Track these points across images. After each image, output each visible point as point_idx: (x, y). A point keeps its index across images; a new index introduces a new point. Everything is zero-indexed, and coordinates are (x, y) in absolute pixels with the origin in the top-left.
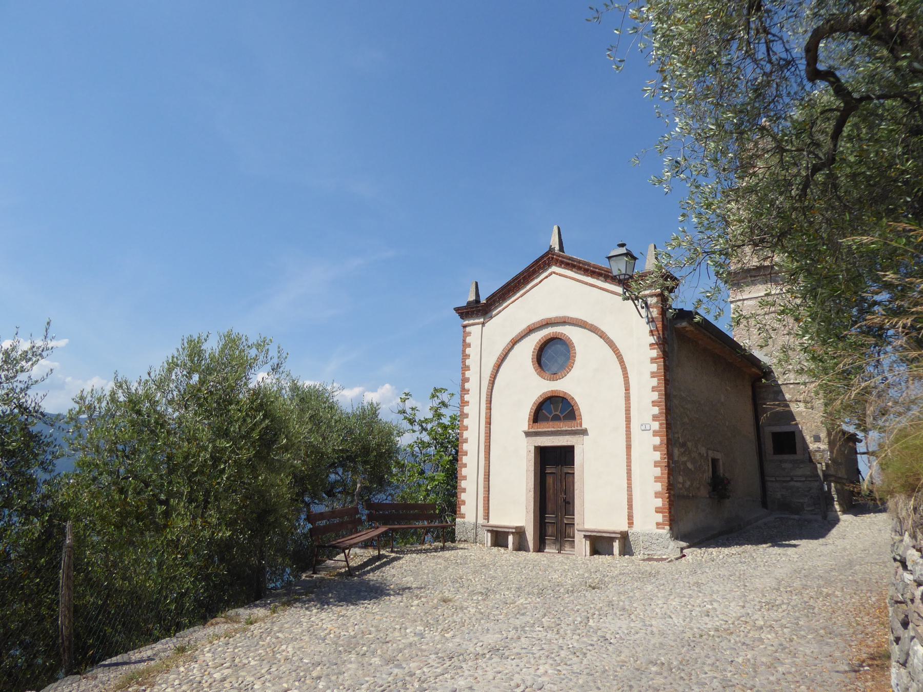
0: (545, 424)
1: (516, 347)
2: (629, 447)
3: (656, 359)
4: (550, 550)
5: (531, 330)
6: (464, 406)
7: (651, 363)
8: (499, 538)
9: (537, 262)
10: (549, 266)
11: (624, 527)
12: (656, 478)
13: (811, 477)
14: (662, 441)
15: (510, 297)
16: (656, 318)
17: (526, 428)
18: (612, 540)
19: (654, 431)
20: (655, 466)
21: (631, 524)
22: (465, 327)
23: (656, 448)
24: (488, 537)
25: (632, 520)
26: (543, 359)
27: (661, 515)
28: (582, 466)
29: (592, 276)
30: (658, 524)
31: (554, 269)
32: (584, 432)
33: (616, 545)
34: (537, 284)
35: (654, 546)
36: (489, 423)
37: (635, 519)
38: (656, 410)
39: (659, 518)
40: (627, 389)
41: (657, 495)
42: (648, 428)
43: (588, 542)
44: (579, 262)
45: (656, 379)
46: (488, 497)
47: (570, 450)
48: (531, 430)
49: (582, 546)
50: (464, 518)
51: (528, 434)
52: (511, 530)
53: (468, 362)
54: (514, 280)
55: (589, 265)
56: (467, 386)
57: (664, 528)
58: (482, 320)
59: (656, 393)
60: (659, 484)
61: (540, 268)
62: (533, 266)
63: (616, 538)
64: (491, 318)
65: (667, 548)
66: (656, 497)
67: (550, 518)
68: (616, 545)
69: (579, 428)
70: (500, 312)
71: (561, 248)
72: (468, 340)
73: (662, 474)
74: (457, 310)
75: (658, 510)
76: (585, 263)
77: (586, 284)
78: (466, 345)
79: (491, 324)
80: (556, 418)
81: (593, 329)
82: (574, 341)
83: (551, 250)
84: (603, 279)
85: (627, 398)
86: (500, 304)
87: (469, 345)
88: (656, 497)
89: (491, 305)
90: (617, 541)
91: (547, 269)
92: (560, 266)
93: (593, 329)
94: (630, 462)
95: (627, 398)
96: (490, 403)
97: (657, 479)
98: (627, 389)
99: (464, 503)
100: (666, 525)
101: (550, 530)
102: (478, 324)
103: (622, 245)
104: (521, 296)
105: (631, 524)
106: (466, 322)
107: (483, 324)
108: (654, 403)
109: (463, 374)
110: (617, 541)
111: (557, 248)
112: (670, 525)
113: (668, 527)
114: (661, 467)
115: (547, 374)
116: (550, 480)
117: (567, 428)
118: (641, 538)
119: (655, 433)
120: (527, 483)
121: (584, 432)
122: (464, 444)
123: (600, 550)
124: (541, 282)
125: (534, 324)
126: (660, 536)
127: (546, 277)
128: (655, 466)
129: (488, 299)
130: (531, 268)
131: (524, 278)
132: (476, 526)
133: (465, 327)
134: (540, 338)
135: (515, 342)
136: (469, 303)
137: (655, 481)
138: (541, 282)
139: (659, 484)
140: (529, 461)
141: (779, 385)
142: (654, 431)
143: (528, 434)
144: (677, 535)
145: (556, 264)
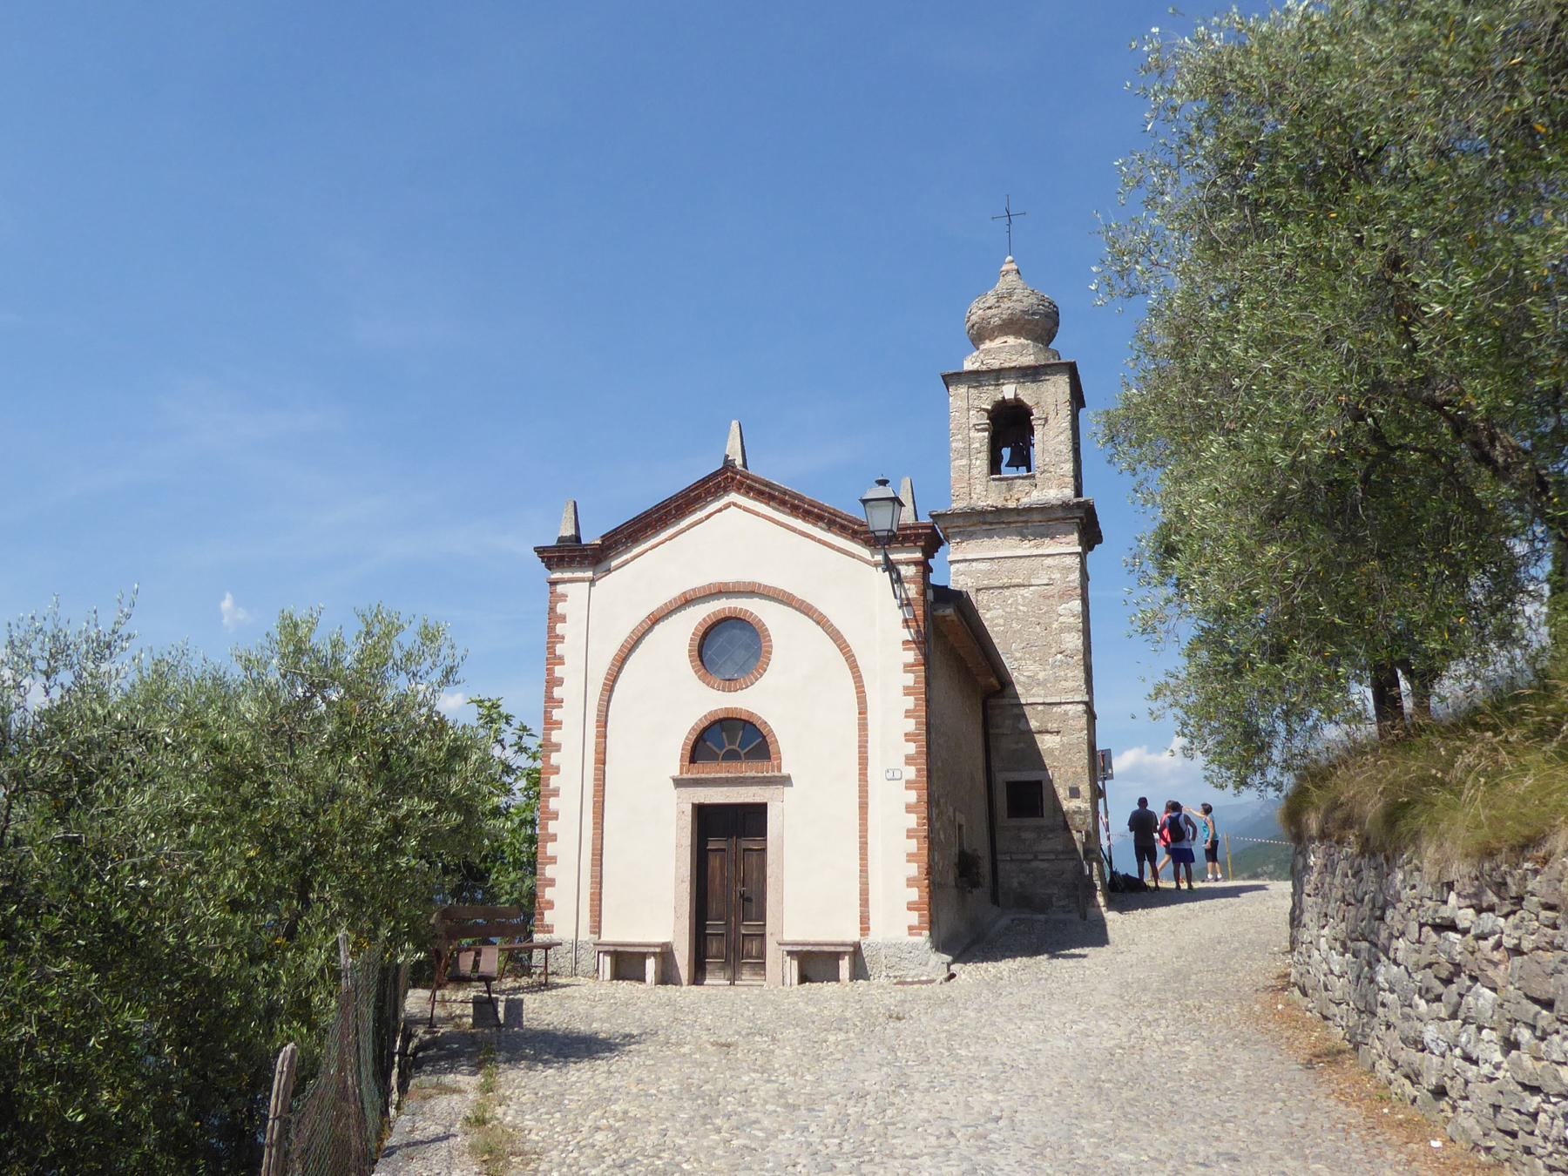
0: (712, 765)
1: (657, 627)
2: (864, 807)
4: (715, 982)
5: (687, 601)
7: (905, 672)
8: (626, 964)
9: (704, 481)
10: (726, 490)
11: (853, 935)
12: (908, 855)
14: (919, 796)
15: (647, 538)
16: (914, 599)
17: (676, 773)
18: (837, 956)
19: (907, 782)
20: (908, 837)
21: (865, 929)
22: (553, 583)
23: (909, 809)
24: (606, 963)
26: (708, 654)
27: (916, 914)
29: (804, 519)
30: (911, 928)
31: (734, 497)
32: (786, 781)
33: (845, 966)
34: (700, 521)
35: (903, 963)
36: (601, 761)
37: (872, 924)
38: (911, 748)
39: (914, 918)
40: (863, 712)
41: (911, 882)
42: (897, 775)
43: (795, 963)
44: (785, 492)
45: (912, 698)
46: (600, 894)
47: (761, 809)
48: (685, 776)
49: (781, 968)
50: (550, 932)
51: (679, 783)
52: (652, 950)
53: (560, 649)
54: (658, 508)
55: (801, 499)
56: (557, 692)
57: (920, 934)
58: (589, 574)
59: (912, 721)
60: (915, 865)
61: (708, 493)
62: (696, 488)
63: (845, 953)
64: (609, 571)
65: (926, 964)
67: (714, 926)
68: (845, 966)
69: (776, 774)
71: (745, 465)
73: (919, 849)
74: (540, 551)
75: (911, 907)
76: (795, 496)
77: (794, 530)
78: (554, 618)
79: (606, 583)
80: (732, 756)
81: (805, 609)
82: (768, 625)
83: (728, 465)
84: (824, 526)
85: (863, 727)
86: (628, 550)
87: (563, 619)
89: (609, 548)
90: (847, 958)
91: (721, 497)
92: (746, 494)
93: (805, 609)
94: (866, 831)
95: (863, 727)
96: (605, 726)
97: (911, 857)
98: (863, 712)
99: (550, 905)
100: (923, 929)
101: (714, 946)
102: (582, 580)
103: (883, 483)
104: (671, 538)
105: (865, 929)
106: (557, 575)
107: (592, 582)
108: (909, 737)
109: (550, 671)
110: (847, 958)
111: (739, 462)
112: (930, 930)
113: (926, 933)
114: (918, 838)
115: (718, 681)
116: (714, 862)
117: (753, 774)
118: (883, 952)
119: (909, 785)
120: (677, 868)
121: (786, 781)
122: (552, 799)
123: (810, 973)
124: (708, 517)
125: (694, 590)
126: (915, 946)
127: (720, 510)
128: (908, 837)
129: (605, 538)
130: (692, 491)
131: (678, 508)
132: (576, 946)
133: (553, 583)
135: (655, 619)
136: (561, 539)
137: (908, 861)
138: (708, 517)
139: (915, 865)
140: (680, 828)
141: (1021, 705)
142: (907, 782)
143: (679, 783)
144: (940, 945)
145: (738, 490)
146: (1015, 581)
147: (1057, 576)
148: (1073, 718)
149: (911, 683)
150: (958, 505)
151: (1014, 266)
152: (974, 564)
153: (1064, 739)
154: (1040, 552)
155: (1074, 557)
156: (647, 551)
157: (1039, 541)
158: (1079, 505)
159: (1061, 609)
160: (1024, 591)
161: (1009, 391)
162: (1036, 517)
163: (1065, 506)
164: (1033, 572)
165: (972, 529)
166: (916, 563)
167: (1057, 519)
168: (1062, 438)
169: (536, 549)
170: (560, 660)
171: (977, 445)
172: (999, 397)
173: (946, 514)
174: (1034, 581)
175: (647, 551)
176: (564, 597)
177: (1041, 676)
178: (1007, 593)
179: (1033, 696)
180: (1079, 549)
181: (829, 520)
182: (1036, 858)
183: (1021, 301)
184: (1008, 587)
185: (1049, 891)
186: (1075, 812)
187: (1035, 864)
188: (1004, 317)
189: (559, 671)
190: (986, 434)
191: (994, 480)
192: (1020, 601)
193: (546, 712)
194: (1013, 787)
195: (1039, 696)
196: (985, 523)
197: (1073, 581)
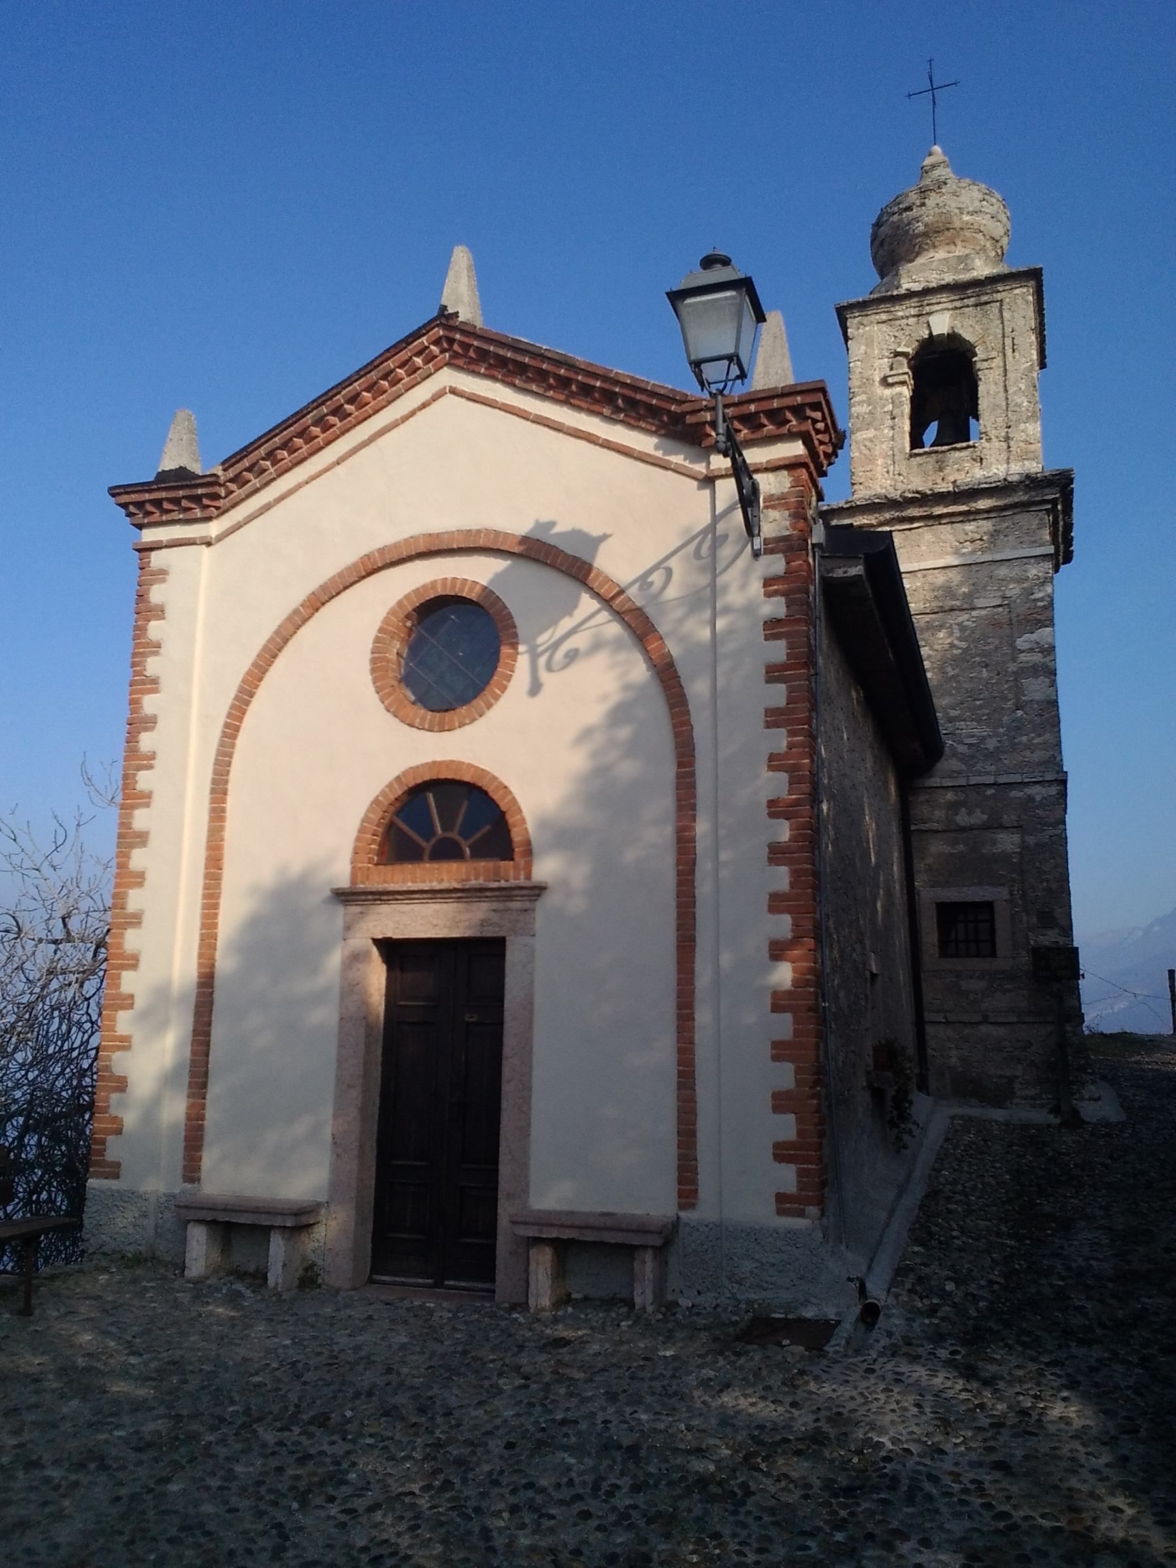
3: (784, 667)
6: (133, 807)
12: (776, 1045)
21: (687, 1192)
25: (694, 1181)
28: (528, 1004)
30: (781, 1198)
31: (447, 377)
34: (395, 425)
50: (117, 1176)
52: (278, 1222)
57: (801, 1214)
60: (789, 1067)
63: (645, 1247)
66: (777, 1109)
69: (522, 881)
70: (267, 507)
72: (156, 594)
83: (445, 318)
88: (777, 1109)
100: (808, 1201)
105: (687, 1192)
106: (150, 535)
109: (135, 704)
126: (791, 1236)
134: (399, 595)
137: (775, 1058)
149: (781, 702)
156: (299, 487)
161: (941, 324)
163: (1030, 482)
166: (791, 466)
169: (114, 492)
170: (152, 685)
175: (299, 487)
176: (162, 573)
177: (991, 744)
179: (980, 774)
181: (627, 399)
182: (985, 1020)
185: (1008, 1073)
186: (1049, 949)
187: (984, 1029)
189: (150, 704)
193: (125, 777)
194: (948, 912)
195: (989, 773)
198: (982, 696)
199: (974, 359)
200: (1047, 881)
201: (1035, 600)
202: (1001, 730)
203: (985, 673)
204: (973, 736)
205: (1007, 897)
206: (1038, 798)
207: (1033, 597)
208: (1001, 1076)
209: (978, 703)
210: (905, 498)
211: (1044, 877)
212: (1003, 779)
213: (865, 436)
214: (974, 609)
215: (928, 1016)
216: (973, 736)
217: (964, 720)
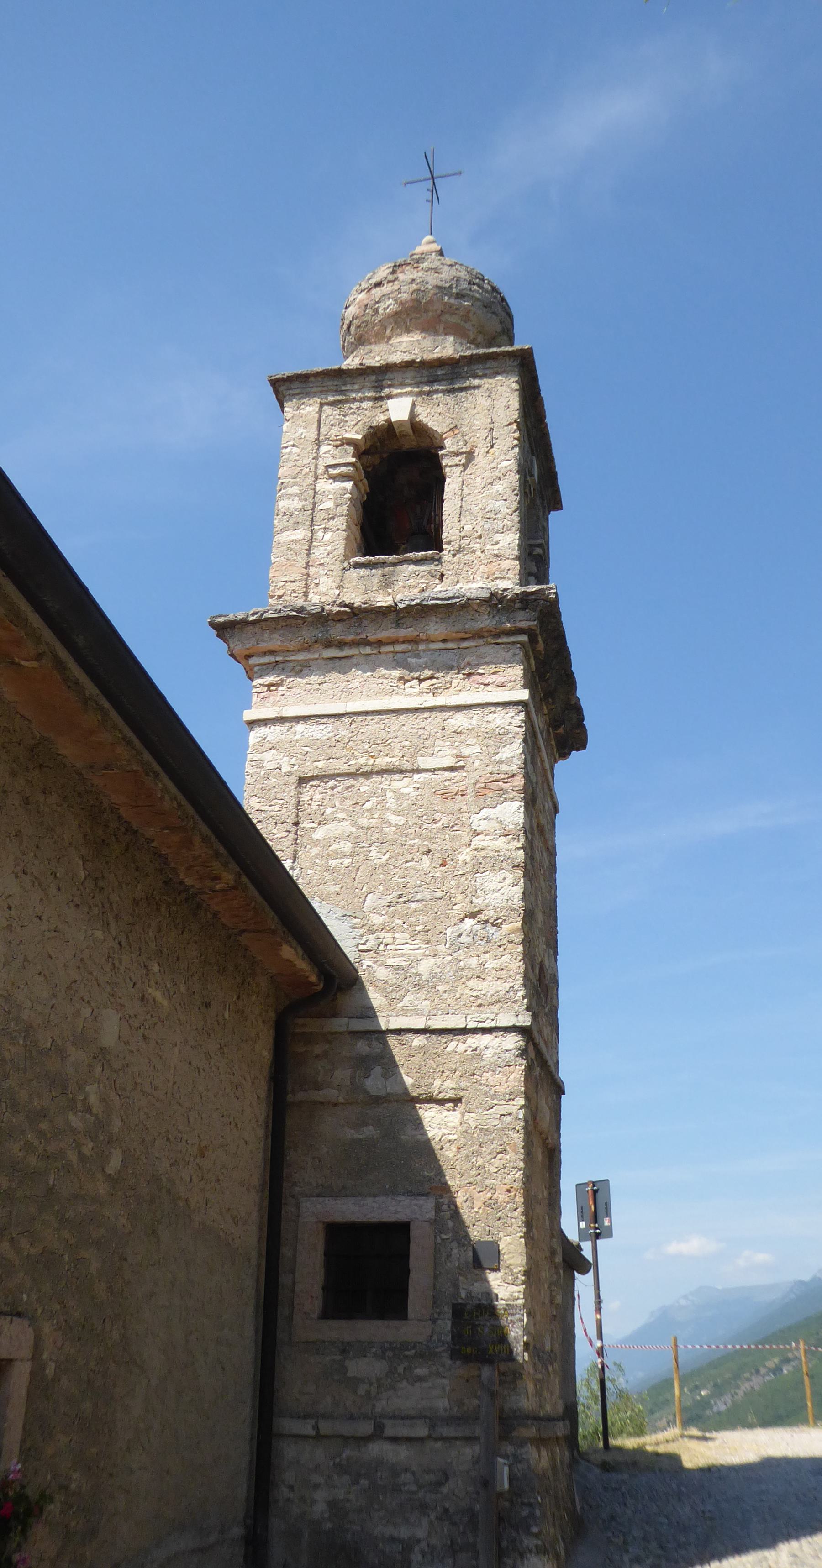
13: (450, 1420)
146: (382, 762)
147: (472, 749)
148: (493, 1068)
150: (272, 607)
151: (436, 247)
152: (300, 727)
153: (472, 1119)
154: (440, 701)
155: (512, 711)
157: (442, 677)
158: (524, 601)
159: (478, 822)
160: (400, 783)
162: (435, 628)
164: (421, 746)
165: (301, 657)
167: (478, 635)
168: (499, 487)
171: (329, 504)
172: (381, 419)
173: (244, 623)
174: (424, 762)
177: (425, 967)
178: (364, 786)
179: (405, 1012)
180: (524, 695)
182: (378, 1434)
183: (437, 271)
184: (368, 775)
185: (404, 1533)
187: (375, 1449)
188: (404, 296)
190: (349, 485)
191: (357, 566)
192: (392, 803)
195: (417, 1012)
196: (329, 644)
197: (509, 761)
198: (419, 897)
199: (440, 453)
200: (493, 1189)
201: (500, 762)
202: (441, 948)
203: (426, 862)
204: (403, 955)
205: (431, 1215)
206: (488, 1054)
207: (497, 758)
208: (393, 1539)
209: (413, 905)
210: (330, 613)
211: (487, 1182)
212: (438, 1023)
213: (293, 538)
214: (418, 771)
215: (287, 1425)
216: (403, 955)
217: (392, 930)
